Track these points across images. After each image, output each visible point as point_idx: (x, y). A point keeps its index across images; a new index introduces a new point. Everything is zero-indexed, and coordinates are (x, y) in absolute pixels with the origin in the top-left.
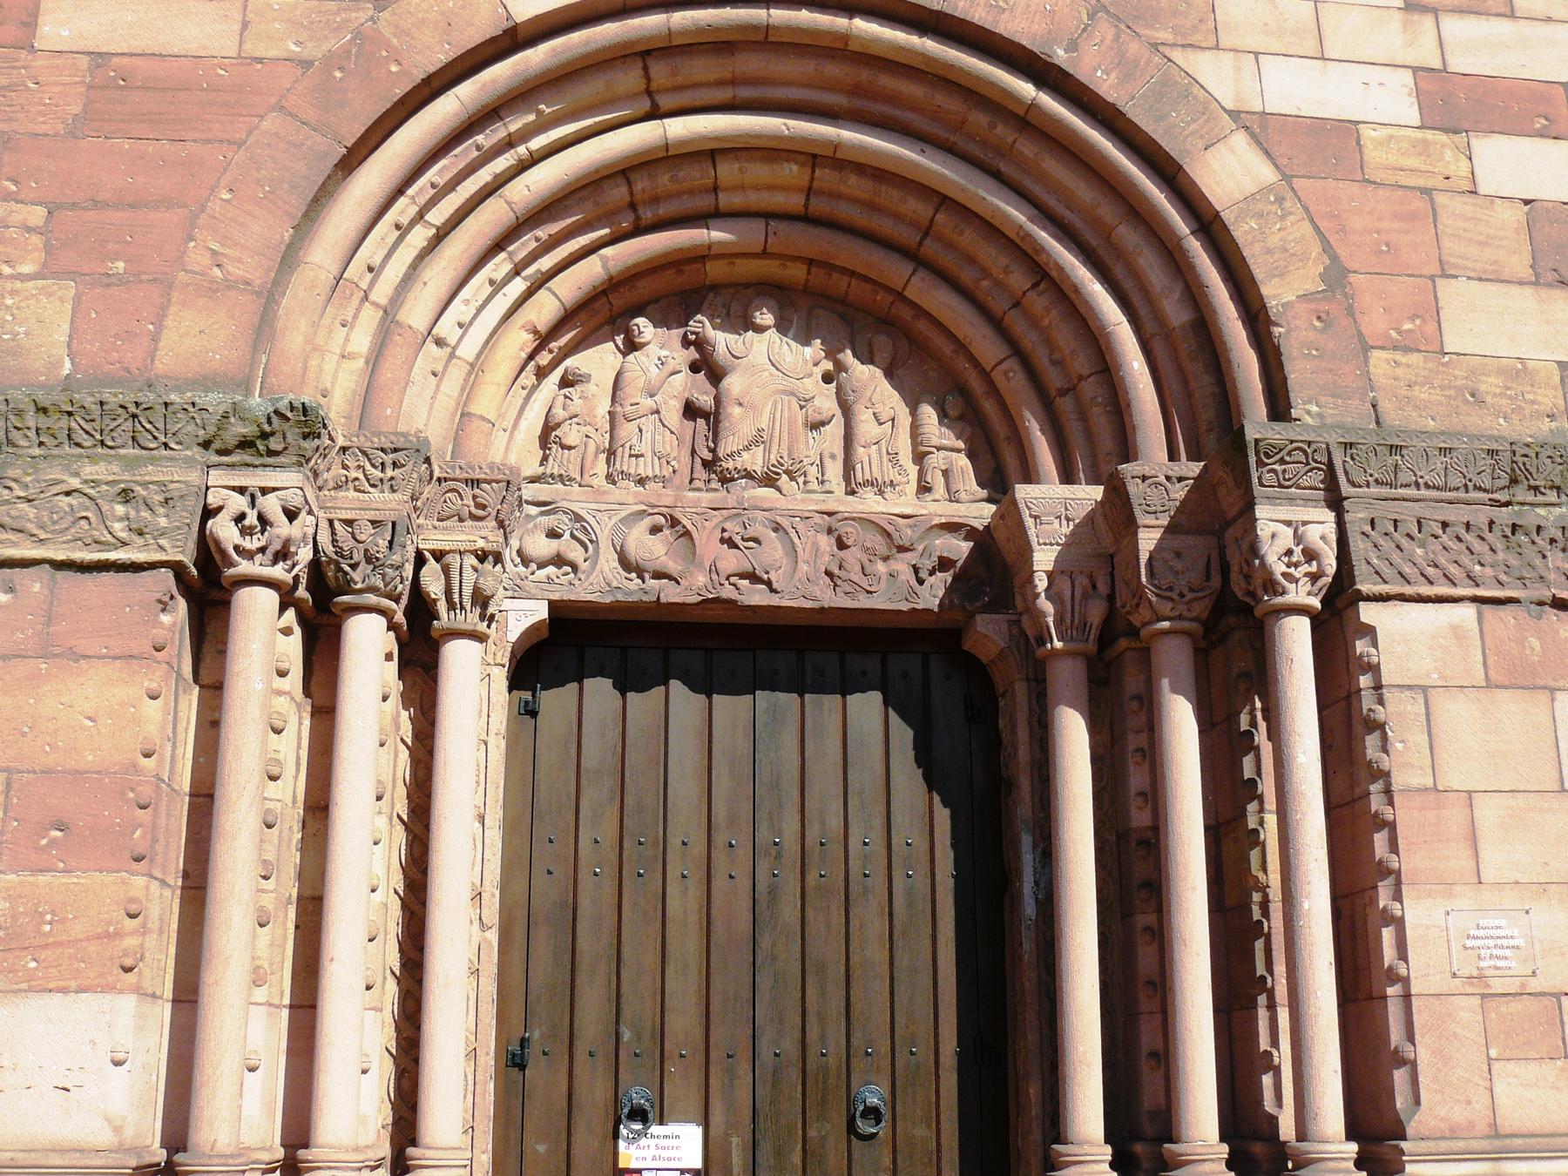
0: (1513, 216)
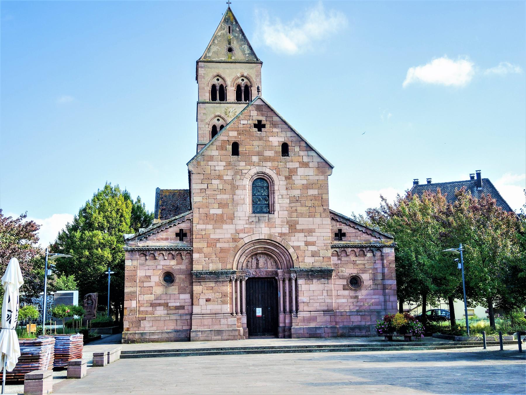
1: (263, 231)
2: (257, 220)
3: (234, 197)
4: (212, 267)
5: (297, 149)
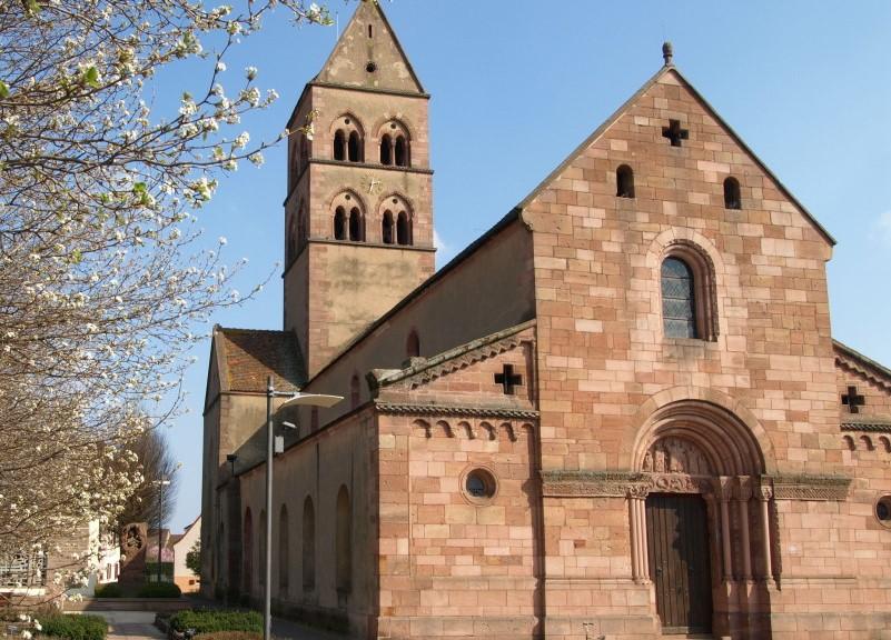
0: (799, 436)
1: (695, 384)
2: (682, 356)
3: (629, 294)
4: (585, 462)
5: (757, 193)
